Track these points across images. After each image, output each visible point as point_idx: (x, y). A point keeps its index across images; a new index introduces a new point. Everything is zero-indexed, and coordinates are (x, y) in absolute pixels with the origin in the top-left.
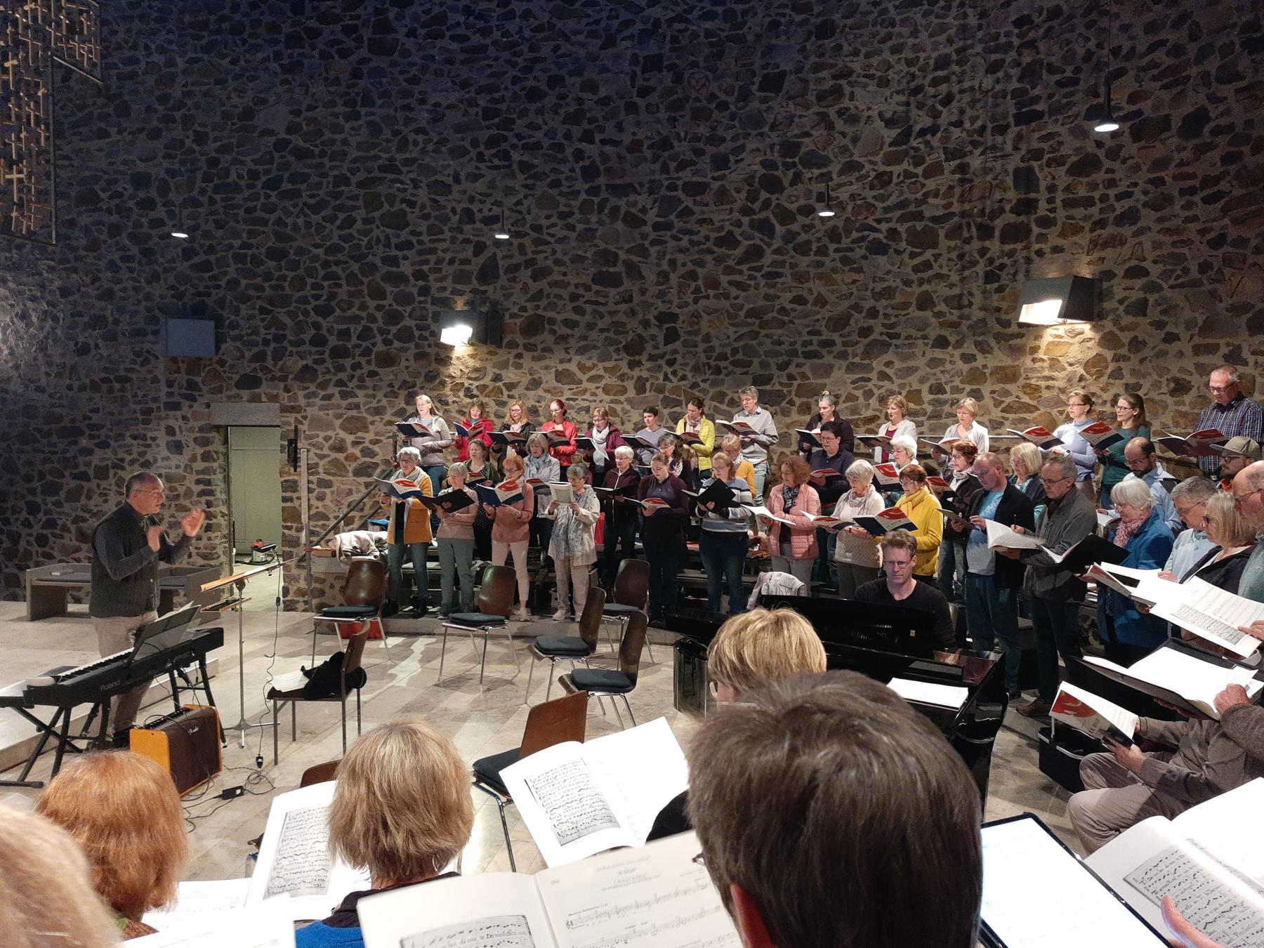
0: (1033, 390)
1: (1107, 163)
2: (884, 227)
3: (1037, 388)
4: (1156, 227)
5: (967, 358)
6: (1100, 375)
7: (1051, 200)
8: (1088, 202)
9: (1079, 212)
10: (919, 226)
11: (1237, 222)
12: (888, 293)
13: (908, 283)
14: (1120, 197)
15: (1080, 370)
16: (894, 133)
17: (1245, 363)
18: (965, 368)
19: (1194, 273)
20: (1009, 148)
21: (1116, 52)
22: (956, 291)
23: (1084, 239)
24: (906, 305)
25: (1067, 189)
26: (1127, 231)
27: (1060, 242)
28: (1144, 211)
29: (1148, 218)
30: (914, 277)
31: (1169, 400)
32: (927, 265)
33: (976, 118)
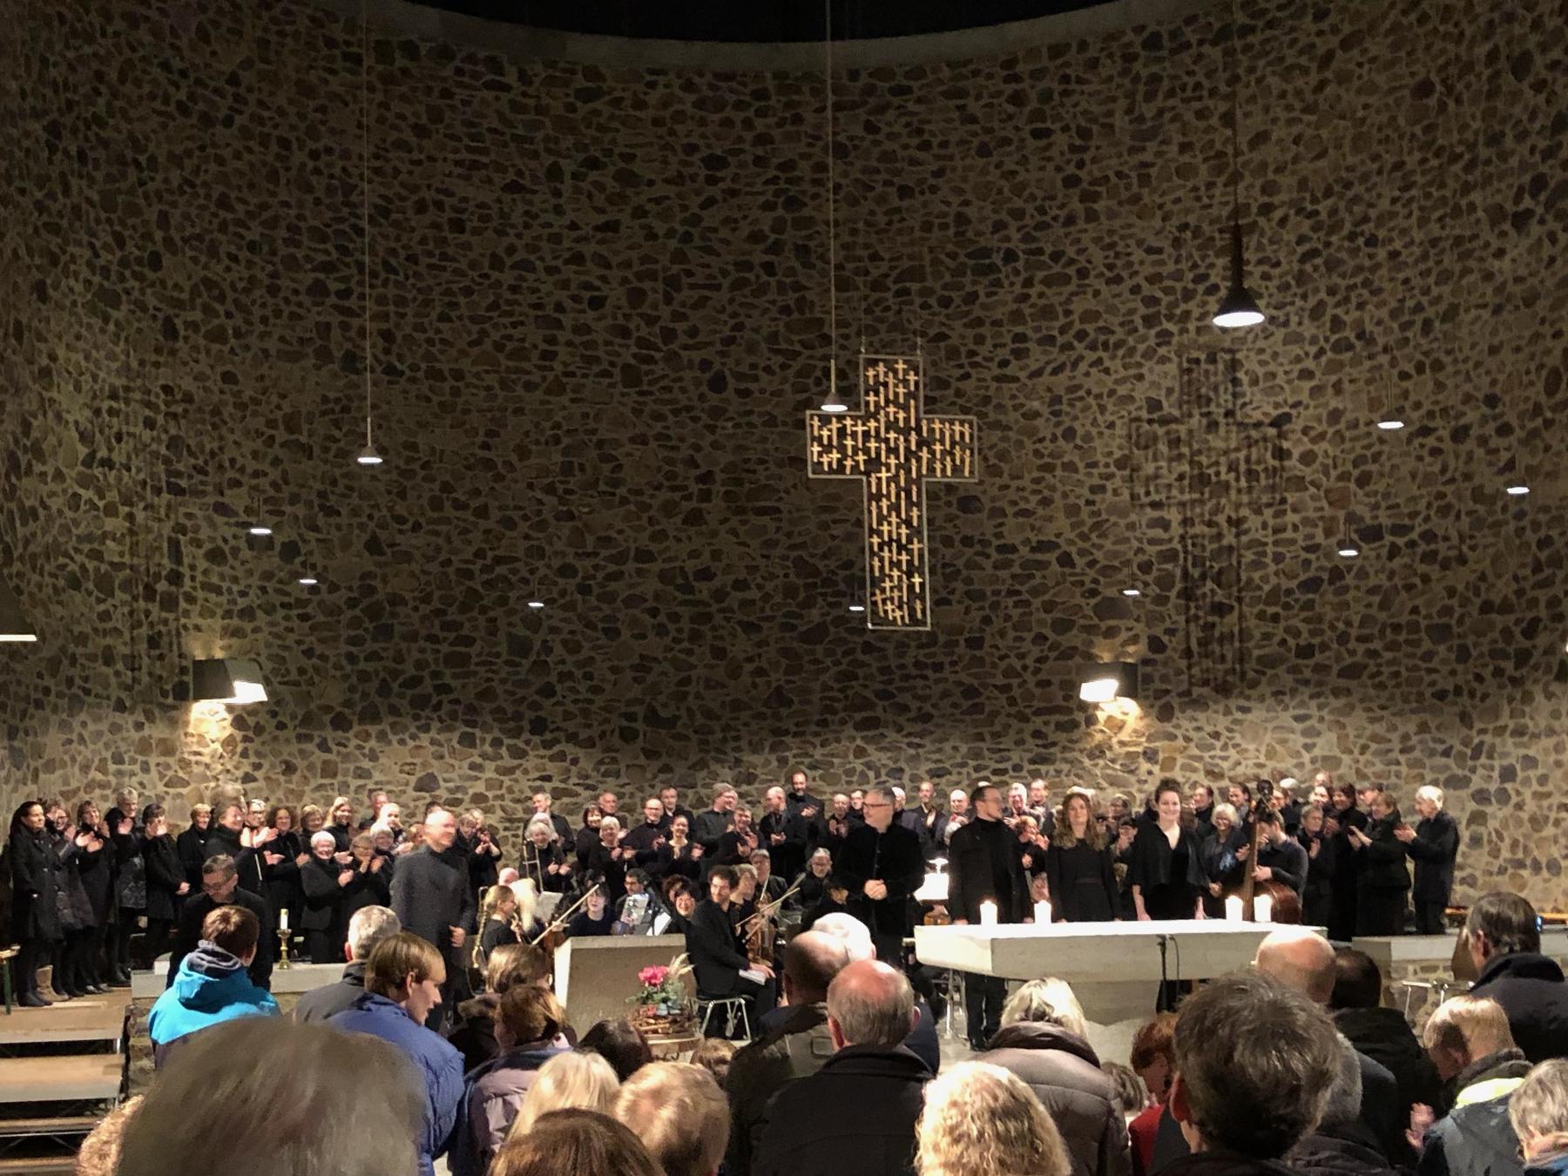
0: (184, 764)
1: (231, 560)
2: (78, 558)
3: (189, 764)
4: (267, 629)
5: (139, 726)
6: (233, 753)
7: (193, 578)
8: (218, 591)
9: (213, 597)
10: (104, 568)
11: (321, 641)
12: (82, 639)
13: (95, 630)
14: (243, 594)
15: (217, 746)
16: (83, 451)
17: (329, 750)
18: (136, 736)
19: (294, 676)
20: (163, 512)
21: (233, 461)
22: (127, 651)
23: (218, 623)
24: (92, 658)
25: (205, 572)
26: (248, 626)
27: (199, 621)
28: (259, 613)
29: (262, 619)
30: (101, 626)
31: (282, 778)
32: (105, 616)
33: (139, 470)
